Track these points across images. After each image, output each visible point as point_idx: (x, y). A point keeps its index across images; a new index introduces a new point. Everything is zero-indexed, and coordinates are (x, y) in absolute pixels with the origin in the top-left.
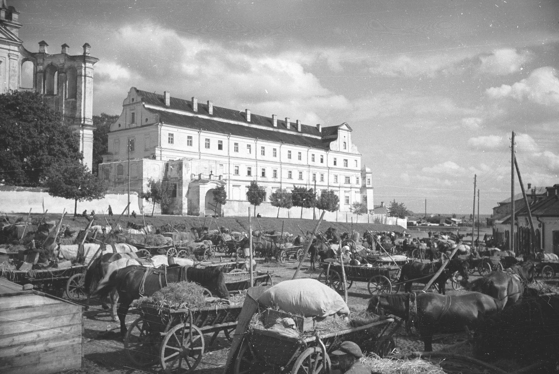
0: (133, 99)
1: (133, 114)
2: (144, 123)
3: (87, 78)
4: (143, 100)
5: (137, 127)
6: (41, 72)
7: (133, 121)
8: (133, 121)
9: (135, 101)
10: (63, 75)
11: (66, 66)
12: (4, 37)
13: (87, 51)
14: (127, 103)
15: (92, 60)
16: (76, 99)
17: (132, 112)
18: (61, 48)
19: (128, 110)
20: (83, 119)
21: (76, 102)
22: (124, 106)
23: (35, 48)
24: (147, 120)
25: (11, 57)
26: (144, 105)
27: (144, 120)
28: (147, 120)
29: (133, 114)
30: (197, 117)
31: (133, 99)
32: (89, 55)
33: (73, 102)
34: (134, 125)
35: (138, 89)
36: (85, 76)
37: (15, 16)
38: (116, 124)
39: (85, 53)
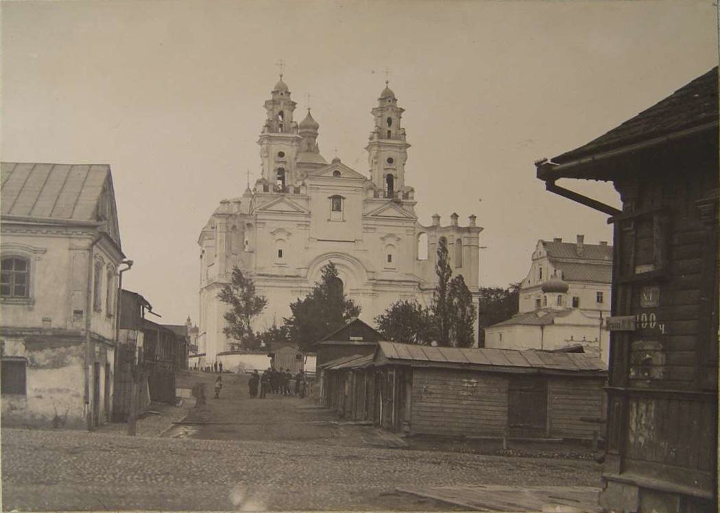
12: (402, 216)
14: (535, 257)
17: (540, 267)
19: (536, 265)
22: (533, 260)
29: (541, 269)
31: (540, 253)
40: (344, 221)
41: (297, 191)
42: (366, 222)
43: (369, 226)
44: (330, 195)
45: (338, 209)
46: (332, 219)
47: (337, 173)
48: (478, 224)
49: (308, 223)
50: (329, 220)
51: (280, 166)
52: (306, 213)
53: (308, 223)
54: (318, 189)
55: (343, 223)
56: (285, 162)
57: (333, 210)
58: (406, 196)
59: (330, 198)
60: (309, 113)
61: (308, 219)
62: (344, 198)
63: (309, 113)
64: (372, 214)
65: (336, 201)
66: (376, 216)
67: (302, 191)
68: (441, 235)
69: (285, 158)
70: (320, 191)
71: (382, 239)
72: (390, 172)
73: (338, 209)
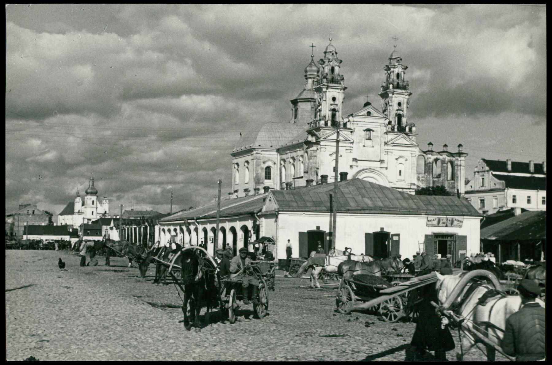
4: (491, 169)
6: (430, 163)
10: (445, 165)
11: (446, 160)
12: (408, 143)
15: (465, 155)
16: (454, 181)
17: (483, 177)
21: (454, 183)
25: (412, 155)
26: (492, 173)
30: (534, 177)
32: (462, 152)
33: (452, 183)
34: (483, 188)
35: (486, 159)
36: (460, 166)
37: (414, 129)
40: (373, 147)
41: (345, 125)
42: (386, 147)
43: (388, 151)
44: (365, 128)
45: (369, 139)
49: (352, 148)
50: (364, 146)
51: (333, 107)
52: (352, 141)
53: (352, 148)
54: (358, 124)
56: (337, 105)
57: (366, 139)
58: (410, 130)
59: (364, 131)
60: (312, 60)
61: (351, 145)
62: (373, 131)
63: (312, 60)
64: (391, 142)
65: (368, 133)
66: (393, 143)
67: (349, 125)
68: (435, 157)
70: (358, 125)
71: (397, 159)
72: (401, 112)
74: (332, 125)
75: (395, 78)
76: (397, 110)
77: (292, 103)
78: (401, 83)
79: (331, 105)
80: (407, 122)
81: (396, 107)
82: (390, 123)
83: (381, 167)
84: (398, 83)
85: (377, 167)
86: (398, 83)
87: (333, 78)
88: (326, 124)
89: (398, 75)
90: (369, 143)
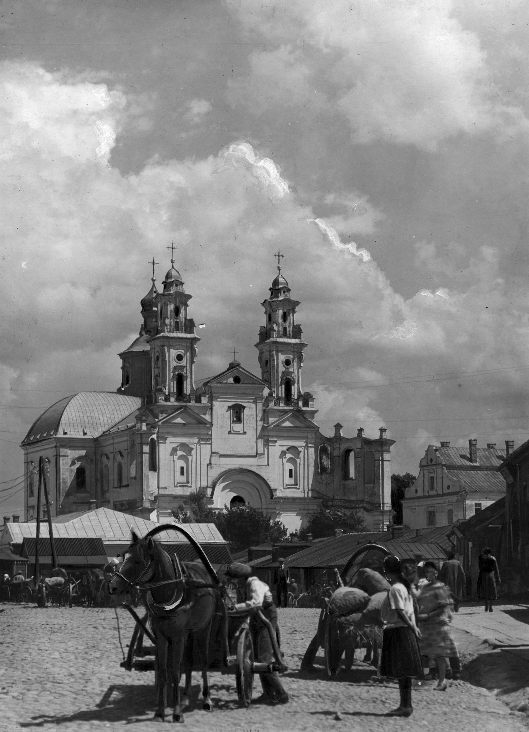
0: (431, 460)
1: (432, 478)
2: (446, 491)
3: (385, 463)
5: (438, 495)
7: (432, 488)
8: (432, 488)
9: (433, 463)
13: (384, 434)
14: (424, 463)
18: (357, 431)
19: (426, 472)
20: (382, 505)
22: (421, 466)
23: (329, 433)
24: (449, 487)
27: (445, 487)
28: (449, 487)
34: (433, 493)
38: (412, 489)
39: (381, 436)
40: (245, 433)
44: (231, 404)
46: (232, 432)
47: (237, 380)
48: (387, 436)
50: (230, 433)
55: (244, 436)
58: (306, 404)
59: (229, 408)
60: (154, 284)
63: (154, 284)
69: (183, 363)
73: (238, 419)
74: (177, 400)
75: (280, 320)
76: (283, 372)
77: (121, 358)
78: (289, 329)
79: (175, 368)
80: (299, 392)
81: (282, 368)
82: (271, 394)
83: (258, 465)
84: (285, 329)
85: (252, 466)
86: (285, 329)
87: (177, 323)
88: (167, 399)
89: (285, 317)
90: (238, 427)
